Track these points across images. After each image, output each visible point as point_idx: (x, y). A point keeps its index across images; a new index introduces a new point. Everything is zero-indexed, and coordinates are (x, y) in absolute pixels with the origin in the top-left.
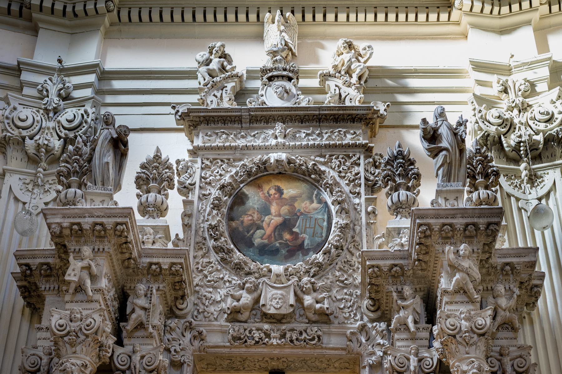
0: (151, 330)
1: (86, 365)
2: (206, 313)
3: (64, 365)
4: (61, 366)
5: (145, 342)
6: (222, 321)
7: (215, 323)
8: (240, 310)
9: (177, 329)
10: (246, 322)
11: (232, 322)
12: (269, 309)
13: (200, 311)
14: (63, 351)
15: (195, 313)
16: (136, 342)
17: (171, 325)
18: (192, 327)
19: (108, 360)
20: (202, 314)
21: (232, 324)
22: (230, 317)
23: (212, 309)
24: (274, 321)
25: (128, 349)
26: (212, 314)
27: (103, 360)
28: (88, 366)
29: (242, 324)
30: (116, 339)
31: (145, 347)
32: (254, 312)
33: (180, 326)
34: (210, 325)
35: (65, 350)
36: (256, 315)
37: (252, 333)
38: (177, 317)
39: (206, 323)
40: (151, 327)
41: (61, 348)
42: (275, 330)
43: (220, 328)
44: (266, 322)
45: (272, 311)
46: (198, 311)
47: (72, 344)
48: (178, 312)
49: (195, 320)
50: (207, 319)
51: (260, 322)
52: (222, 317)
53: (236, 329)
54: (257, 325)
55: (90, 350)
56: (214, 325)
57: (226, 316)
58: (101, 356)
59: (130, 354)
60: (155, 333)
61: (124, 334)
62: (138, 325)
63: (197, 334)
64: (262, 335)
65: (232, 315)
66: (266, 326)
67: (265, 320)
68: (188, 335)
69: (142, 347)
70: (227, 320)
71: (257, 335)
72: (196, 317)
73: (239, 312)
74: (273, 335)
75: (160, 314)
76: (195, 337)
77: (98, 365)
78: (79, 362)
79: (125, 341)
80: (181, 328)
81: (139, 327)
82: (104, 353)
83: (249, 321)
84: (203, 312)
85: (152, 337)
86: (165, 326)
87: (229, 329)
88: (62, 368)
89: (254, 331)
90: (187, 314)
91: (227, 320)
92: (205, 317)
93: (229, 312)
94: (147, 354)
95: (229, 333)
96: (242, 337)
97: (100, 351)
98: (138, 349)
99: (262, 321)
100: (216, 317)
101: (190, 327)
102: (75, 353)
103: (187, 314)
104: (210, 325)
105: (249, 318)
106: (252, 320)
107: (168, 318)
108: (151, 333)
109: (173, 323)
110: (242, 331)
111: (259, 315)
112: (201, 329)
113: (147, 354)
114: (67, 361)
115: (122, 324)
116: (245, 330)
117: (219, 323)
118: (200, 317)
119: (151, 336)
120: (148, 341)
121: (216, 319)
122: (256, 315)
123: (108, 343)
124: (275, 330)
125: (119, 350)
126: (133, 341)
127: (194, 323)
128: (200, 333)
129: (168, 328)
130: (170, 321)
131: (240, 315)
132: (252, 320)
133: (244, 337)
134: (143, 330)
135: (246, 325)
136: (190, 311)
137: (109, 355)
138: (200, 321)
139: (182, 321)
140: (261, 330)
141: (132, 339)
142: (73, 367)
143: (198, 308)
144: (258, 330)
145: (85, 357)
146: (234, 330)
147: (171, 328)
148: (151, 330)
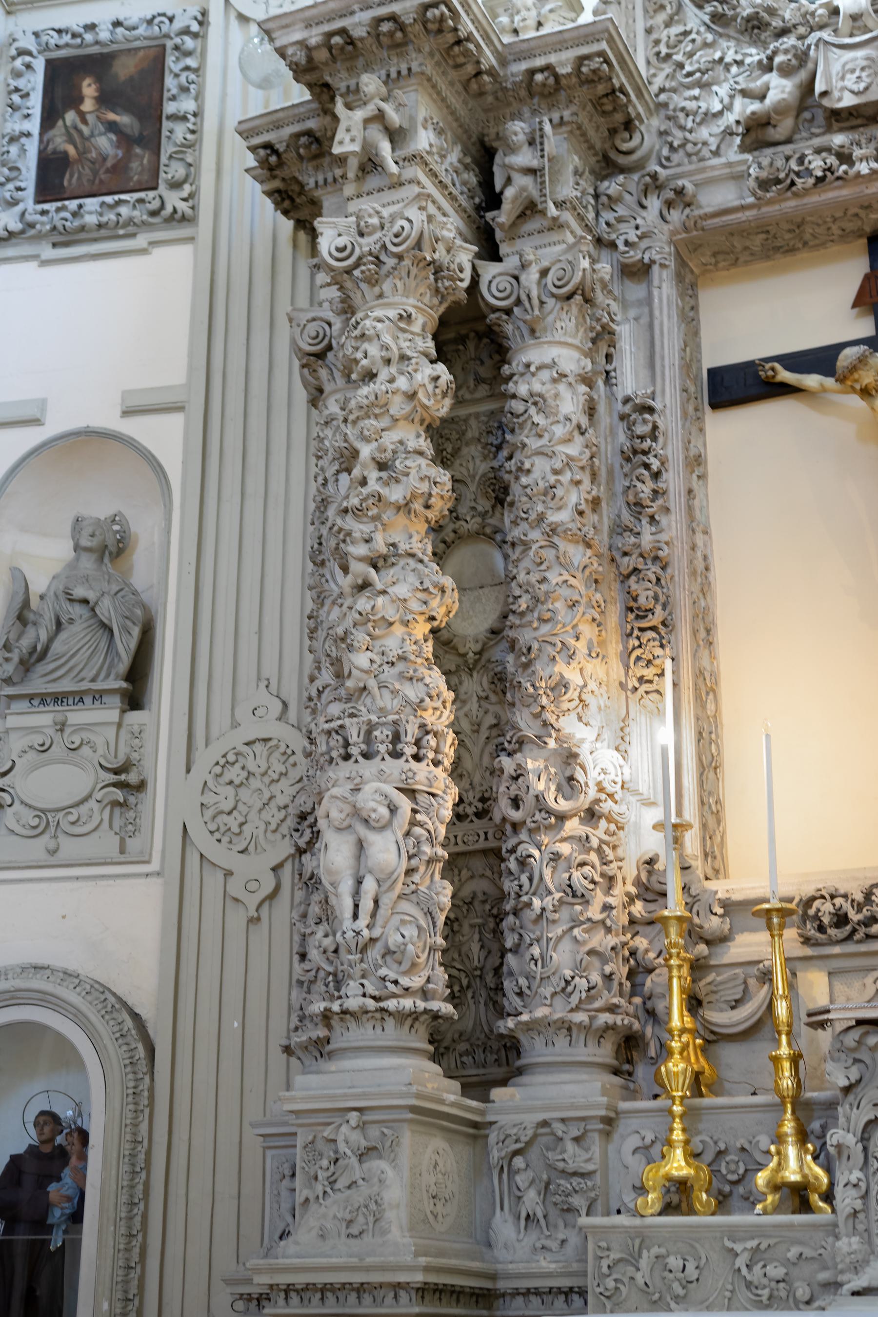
0: (552, 211)
1: (409, 316)
2: (689, 147)
3: (360, 327)
4: (355, 328)
5: (546, 241)
6: (733, 154)
7: (715, 161)
8: (769, 117)
9: (627, 197)
10: (789, 141)
11: (756, 149)
12: (840, 99)
13: (676, 144)
14: (357, 298)
15: (665, 152)
16: (527, 247)
17: (610, 192)
18: (659, 183)
19: (463, 296)
20: (681, 152)
21: (756, 153)
22: (748, 141)
23: (704, 133)
24: (859, 121)
25: (511, 263)
26: (705, 143)
27: (450, 299)
28: (414, 315)
29: (780, 148)
30: (475, 248)
31: (548, 250)
32: (807, 115)
33: (633, 188)
34: (703, 170)
35: (359, 295)
36: (812, 120)
37: (806, 161)
38: (623, 170)
39: (693, 167)
40: (551, 205)
41: (351, 294)
42: (863, 141)
43: (727, 170)
44: (841, 130)
45: (848, 101)
46: (671, 145)
47: (373, 281)
48: (622, 160)
49: (664, 167)
50: (694, 158)
51: (823, 134)
52: (730, 145)
53: (765, 162)
54: (817, 142)
55: (413, 284)
56: (713, 168)
57: (738, 140)
58: (442, 290)
59: (516, 272)
60: (567, 217)
61: (499, 235)
62: (527, 208)
63: (671, 195)
64: (832, 160)
65: (753, 135)
66: (838, 139)
67: (836, 126)
68: (654, 204)
69: (540, 252)
70: (743, 149)
71: (817, 164)
72: (668, 159)
73: (768, 123)
74: (857, 153)
75: (576, 172)
76: (669, 204)
77: (442, 309)
78: (392, 313)
79: (504, 249)
80: (634, 191)
81: (528, 212)
82: (447, 283)
83: (797, 137)
84: (682, 146)
85: (561, 226)
86: (596, 196)
87: (749, 167)
88: (357, 333)
89: (810, 158)
90: (645, 159)
91: (743, 149)
92: (689, 155)
93: (740, 130)
94: (553, 264)
95: (750, 175)
96: (782, 175)
97: (436, 280)
98: (531, 257)
99: (829, 129)
100: (714, 148)
101: (655, 184)
102: (381, 296)
103: (645, 159)
104: (703, 170)
105: (796, 130)
106: (804, 134)
107: (603, 178)
108: (555, 219)
109: (612, 187)
110: (780, 163)
111: (820, 119)
112: (680, 183)
113: (553, 264)
114: (367, 316)
115: (489, 215)
116: (788, 159)
117: (723, 160)
118: (676, 158)
119: (557, 225)
120: (554, 236)
121: (716, 153)
122: (812, 120)
123: (457, 260)
124: (863, 141)
125: (490, 270)
126: (519, 244)
127: (663, 173)
128: (680, 192)
129: (604, 199)
130: (606, 184)
131: (771, 131)
132: (804, 134)
133: (787, 175)
134: (538, 217)
135: (787, 149)
136: (651, 151)
137: (465, 284)
138: (679, 165)
139: (636, 177)
140: (828, 150)
141: (518, 241)
142: (379, 325)
143: (670, 139)
144: (818, 151)
145: (404, 300)
146: (760, 167)
147: (609, 197)
148: (552, 211)
